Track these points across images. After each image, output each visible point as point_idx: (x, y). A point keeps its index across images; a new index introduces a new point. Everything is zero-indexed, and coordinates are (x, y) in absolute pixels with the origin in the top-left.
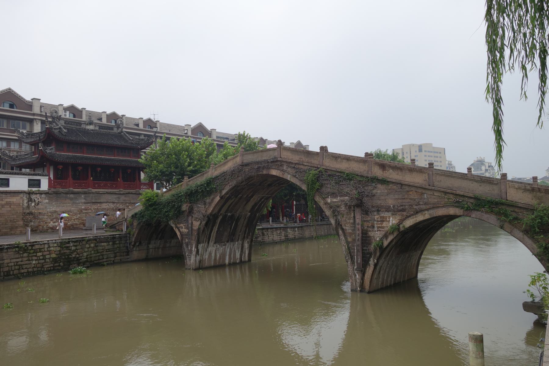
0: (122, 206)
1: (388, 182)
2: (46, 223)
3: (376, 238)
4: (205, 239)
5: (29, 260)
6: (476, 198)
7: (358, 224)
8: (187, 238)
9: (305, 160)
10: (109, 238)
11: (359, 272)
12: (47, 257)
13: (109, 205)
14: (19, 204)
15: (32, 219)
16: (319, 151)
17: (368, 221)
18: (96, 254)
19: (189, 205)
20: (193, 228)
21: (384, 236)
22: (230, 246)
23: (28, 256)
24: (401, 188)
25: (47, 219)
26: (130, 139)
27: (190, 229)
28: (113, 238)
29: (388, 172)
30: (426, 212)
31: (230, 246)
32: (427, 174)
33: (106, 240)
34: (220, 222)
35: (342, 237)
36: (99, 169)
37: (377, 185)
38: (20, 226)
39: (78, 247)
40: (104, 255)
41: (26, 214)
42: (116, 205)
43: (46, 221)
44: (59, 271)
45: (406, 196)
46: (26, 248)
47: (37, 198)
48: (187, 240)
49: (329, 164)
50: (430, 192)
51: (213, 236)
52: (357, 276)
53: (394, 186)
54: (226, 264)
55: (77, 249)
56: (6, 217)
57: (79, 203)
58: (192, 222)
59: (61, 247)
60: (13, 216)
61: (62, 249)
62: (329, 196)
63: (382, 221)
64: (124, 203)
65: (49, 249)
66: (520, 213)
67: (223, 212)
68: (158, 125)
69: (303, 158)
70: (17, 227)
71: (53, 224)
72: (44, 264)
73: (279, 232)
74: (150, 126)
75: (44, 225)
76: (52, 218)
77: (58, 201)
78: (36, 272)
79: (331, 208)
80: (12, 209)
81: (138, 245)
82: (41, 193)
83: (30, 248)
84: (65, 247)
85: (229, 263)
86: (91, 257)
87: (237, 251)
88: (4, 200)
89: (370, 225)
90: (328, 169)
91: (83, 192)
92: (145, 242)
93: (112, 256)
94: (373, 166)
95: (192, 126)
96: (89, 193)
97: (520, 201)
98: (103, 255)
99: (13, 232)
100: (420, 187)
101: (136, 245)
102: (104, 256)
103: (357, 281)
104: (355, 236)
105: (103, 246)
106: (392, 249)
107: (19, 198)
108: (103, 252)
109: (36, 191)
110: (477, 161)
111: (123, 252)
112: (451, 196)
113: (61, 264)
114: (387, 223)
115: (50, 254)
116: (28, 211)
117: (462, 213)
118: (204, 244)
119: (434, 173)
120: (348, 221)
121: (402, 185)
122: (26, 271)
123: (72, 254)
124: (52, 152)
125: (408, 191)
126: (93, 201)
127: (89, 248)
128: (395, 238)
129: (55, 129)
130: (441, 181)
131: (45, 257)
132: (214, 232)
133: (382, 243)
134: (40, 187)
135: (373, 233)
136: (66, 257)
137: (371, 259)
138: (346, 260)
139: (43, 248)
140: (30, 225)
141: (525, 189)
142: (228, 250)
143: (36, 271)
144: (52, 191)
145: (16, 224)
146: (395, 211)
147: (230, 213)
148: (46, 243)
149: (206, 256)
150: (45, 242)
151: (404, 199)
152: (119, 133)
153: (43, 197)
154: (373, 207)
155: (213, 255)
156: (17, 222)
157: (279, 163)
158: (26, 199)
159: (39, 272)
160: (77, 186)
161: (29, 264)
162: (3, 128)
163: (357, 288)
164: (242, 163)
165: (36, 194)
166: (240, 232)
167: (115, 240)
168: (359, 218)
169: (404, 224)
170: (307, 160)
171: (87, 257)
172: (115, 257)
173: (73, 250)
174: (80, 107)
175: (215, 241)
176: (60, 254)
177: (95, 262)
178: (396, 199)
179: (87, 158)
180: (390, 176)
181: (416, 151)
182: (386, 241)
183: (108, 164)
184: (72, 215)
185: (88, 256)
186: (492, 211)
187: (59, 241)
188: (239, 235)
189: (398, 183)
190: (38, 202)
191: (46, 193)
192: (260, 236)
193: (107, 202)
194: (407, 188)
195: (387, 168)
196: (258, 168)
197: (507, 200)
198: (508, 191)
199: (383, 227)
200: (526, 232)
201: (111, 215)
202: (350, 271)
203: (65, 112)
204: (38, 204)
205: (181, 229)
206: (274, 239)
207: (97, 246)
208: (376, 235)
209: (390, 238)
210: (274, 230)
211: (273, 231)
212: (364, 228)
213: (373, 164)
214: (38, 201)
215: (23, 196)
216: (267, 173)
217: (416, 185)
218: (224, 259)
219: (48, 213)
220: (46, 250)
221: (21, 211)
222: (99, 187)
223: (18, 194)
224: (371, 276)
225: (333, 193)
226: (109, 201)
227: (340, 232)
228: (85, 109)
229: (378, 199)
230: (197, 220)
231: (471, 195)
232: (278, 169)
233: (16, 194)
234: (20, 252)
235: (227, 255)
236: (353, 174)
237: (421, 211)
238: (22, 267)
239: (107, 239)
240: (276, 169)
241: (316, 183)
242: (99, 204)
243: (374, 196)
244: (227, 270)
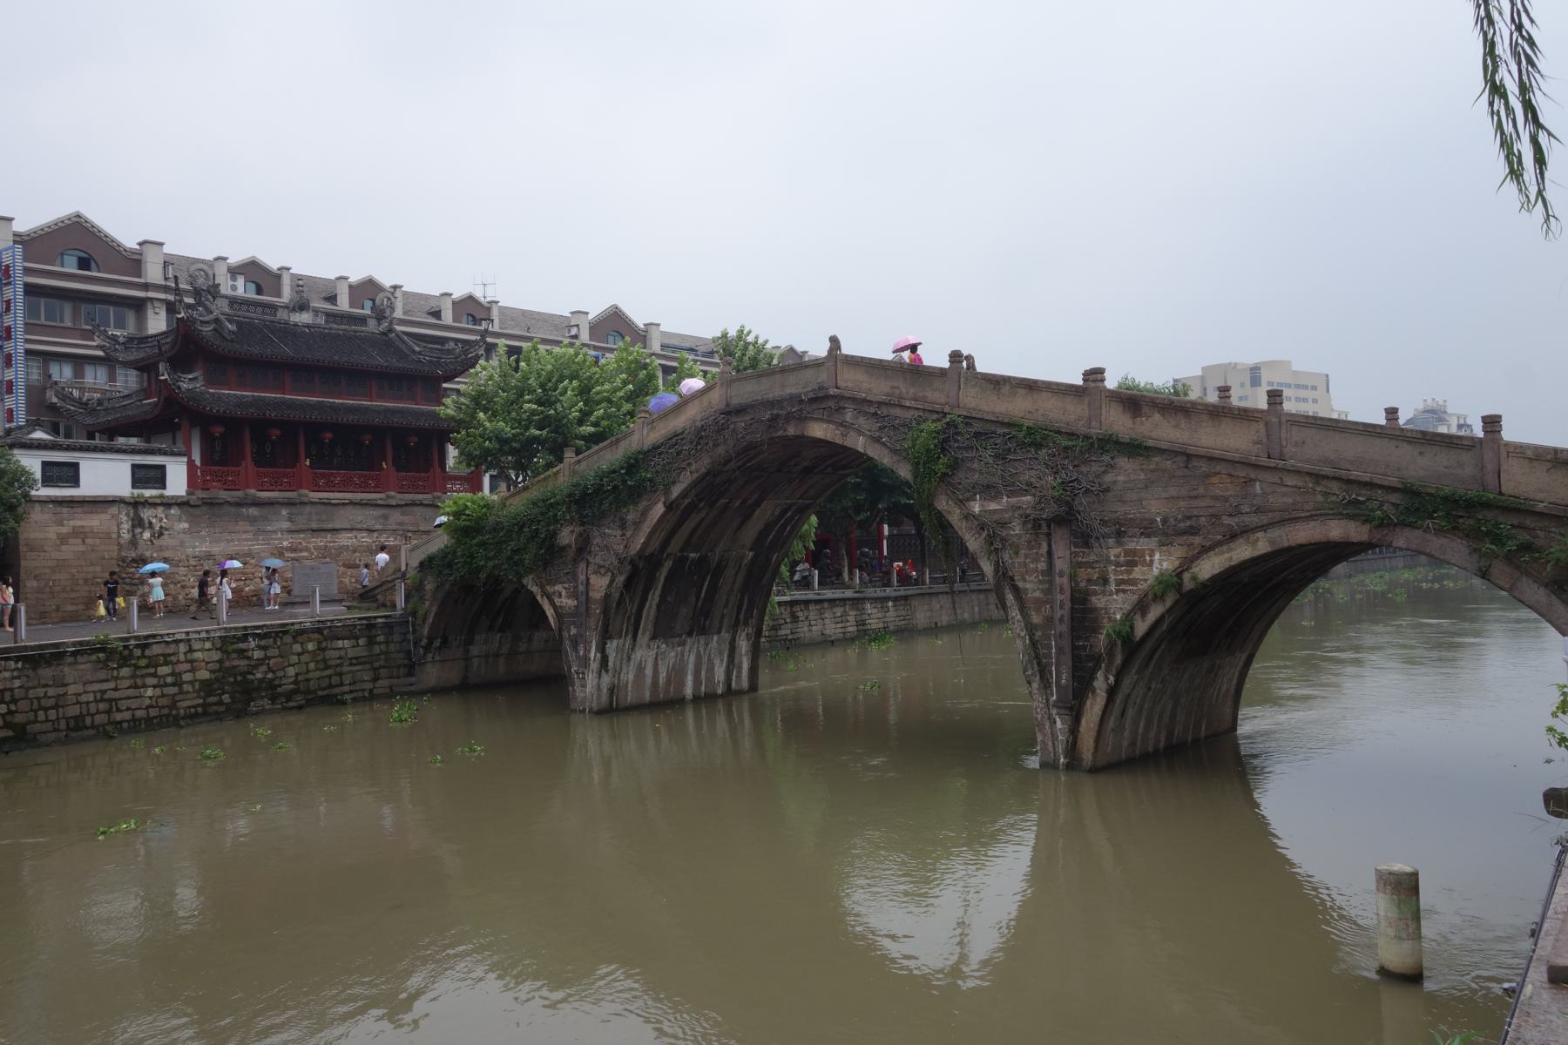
1: (1147, 448)
2: (183, 587)
3: (1114, 613)
4: (625, 625)
5: (136, 687)
6: (1407, 491)
7: (1061, 575)
8: (574, 623)
9: (907, 393)
10: (358, 627)
11: (1063, 711)
12: (187, 677)
14: (108, 536)
16: (946, 364)
17: (1089, 565)
18: (323, 670)
19: (578, 529)
20: (591, 594)
21: (1137, 605)
22: (696, 646)
23: (133, 676)
24: (1187, 467)
26: (414, 351)
27: (583, 598)
28: (370, 626)
29: (1147, 419)
30: (1260, 535)
31: (698, 648)
32: (1261, 426)
33: (349, 632)
34: (667, 578)
35: (1015, 613)
37: (1117, 460)
39: (270, 653)
40: (346, 673)
43: (183, 581)
44: (219, 717)
45: (1201, 490)
46: (126, 652)
48: (573, 631)
49: (973, 401)
50: (1273, 478)
51: (647, 617)
52: (1059, 724)
53: (1167, 460)
54: (687, 697)
55: (269, 658)
56: (74, 571)
58: (588, 579)
59: (223, 652)
60: (91, 569)
61: (225, 656)
63: (1132, 564)
65: (189, 656)
66: (1538, 532)
67: (675, 546)
68: (495, 314)
69: (901, 386)
72: (176, 698)
73: (839, 611)
74: (472, 316)
75: (179, 594)
77: (214, 527)
78: (155, 721)
79: (983, 529)
80: (90, 549)
81: (440, 648)
82: (168, 504)
83: (138, 652)
84: (235, 651)
85: (694, 696)
86: (308, 680)
87: (717, 662)
88: (65, 522)
89: (1096, 575)
90: (974, 415)
91: (286, 501)
92: (458, 638)
93: (366, 679)
94: (1103, 407)
95: (590, 317)
97: (1540, 496)
98: (340, 675)
100: (1243, 463)
101: (434, 645)
102: (344, 677)
103: (1058, 737)
104: (1051, 607)
105: (340, 649)
106: (1159, 645)
108: (341, 665)
109: (155, 497)
110: (1425, 412)
111: (399, 667)
112: (1335, 487)
113: (226, 698)
115: (193, 670)
116: (133, 555)
117: (1366, 536)
118: (621, 641)
119: (1283, 420)
120: (1031, 565)
121: (1189, 457)
122: (127, 715)
123: (254, 672)
124: (196, 388)
125: (1207, 476)
126: (314, 526)
127: (302, 654)
128: (1168, 611)
129: (201, 322)
130: (1303, 443)
131: (181, 678)
132: (650, 607)
133: (1132, 628)
134: (164, 487)
136: (239, 678)
137: (1100, 675)
138: (1027, 677)
139: (173, 654)
140: (139, 593)
141: (1556, 459)
142: (692, 659)
143: (155, 717)
144: (198, 498)
146: (1167, 533)
148: (181, 641)
149: (628, 673)
150: (178, 637)
151: (1196, 497)
152: (383, 334)
153: (173, 515)
154: (1103, 523)
155: (649, 671)
157: (831, 403)
159: (164, 719)
161: (136, 697)
162: (61, 325)
163: (1056, 759)
164: (728, 405)
165: (155, 505)
166: (726, 606)
167: (374, 632)
168: (1063, 555)
169: (1195, 570)
170: (912, 391)
171: (297, 678)
172: (375, 680)
173: (258, 660)
174: (273, 264)
175: (654, 632)
176: (219, 670)
177: (320, 693)
178: (1173, 497)
179: (291, 405)
180: (1152, 434)
181: (1242, 385)
182: (1143, 621)
185: (300, 678)
186: (1455, 528)
187: (218, 634)
188: (723, 616)
189: (1176, 453)
190: (161, 527)
191: (181, 503)
192: (786, 623)
193: (352, 529)
194: (1204, 467)
195: (1145, 409)
196: (774, 419)
197: (1501, 493)
198: (1504, 467)
199: (1133, 582)
200: (1556, 587)
202: (1039, 710)
203: (234, 278)
204: (161, 534)
205: (556, 600)
206: (827, 632)
207: (324, 650)
208: (1114, 605)
209: (1155, 612)
210: (826, 605)
211: (823, 608)
212: (1077, 584)
213: (1103, 397)
214: (159, 525)
215: (120, 513)
216: (798, 433)
217: (1230, 455)
218: (682, 684)
219: (188, 561)
220: (182, 657)
221: (115, 555)
222: (330, 487)
224: (1097, 723)
225: (988, 487)
226: (359, 526)
227: (1010, 597)
228: (288, 269)
230: (603, 571)
231: (1393, 481)
232: (829, 422)
234: (110, 664)
235: (689, 672)
236: (1046, 430)
237: (1246, 532)
238: (116, 704)
239: (351, 628)
240: (822, 420)
241: (939, 458)
243: (1107, 490)
244: (690, 713)
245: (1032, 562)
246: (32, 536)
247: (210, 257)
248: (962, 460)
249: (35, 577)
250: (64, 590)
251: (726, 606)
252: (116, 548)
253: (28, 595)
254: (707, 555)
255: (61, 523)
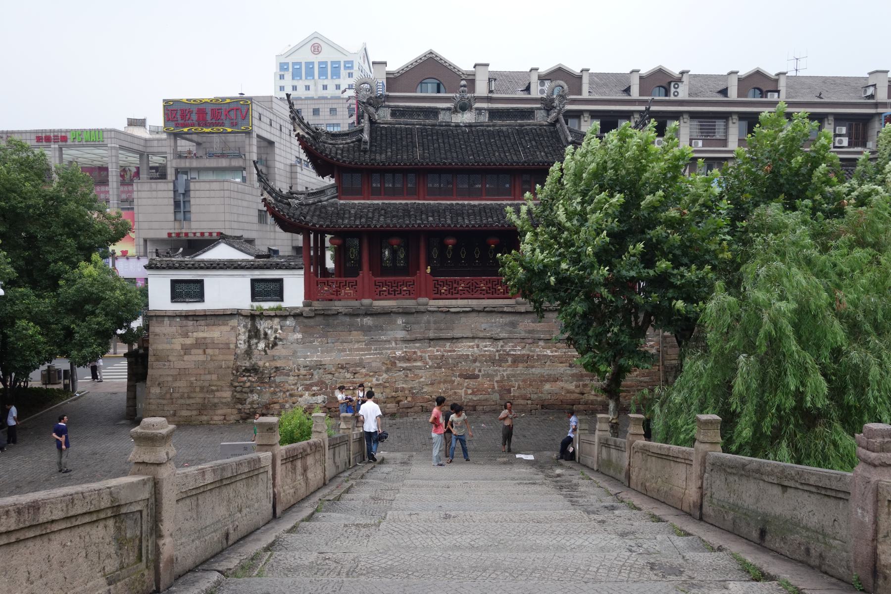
0: (524, 348)
2: (291, 395)
13: (481, 347)
14: (227, 346)
15: (255, 385)
25: (296, 384)
36: (451, 242)
38: (222, 403)
41: (241, 371)
42: (502, 346)
47: (271, 328)
56: (193, 379)
57: (389, 341)
60: (208, 377)
64: (530, 341)
70: (215, 405)
71: (309, 398)
75: (287, 402)
76: (308, 382)
80: (209, 358)
82: (283, 315)
88: (190, 334)
91: (401, 310)
96: (417, 312)
99: (204, 418)
107: (228, 328)
116: (248, 364)
124: (321, 201)
126: (431, 335)
134: (282, 300)
140: (249, 400)
145: (214, 397)
156: (218, 391)
158: (245, 333)
160: (386, 293)
165: (270, 317)
174: (576, 69)
183: (467, 226)
184: (366, 375)
190: (276, 338)
191: (297, 315)
193: (473, 338)
201: (483, 375)
203: (542, 84)
204: (275, 344)
219: (299, 370)
221: (231, 364)
222: (453, 294)
223: (227, 318)
226: (481, 335)
228: (588, 70)
233: (222, 318)
242: (448, 344)
246: (160, 347)
247: (627, 71)
249: (159, 384)
250: (182, 397)
252: (232, 357)
253: (151, 401)
255: (186, 335)
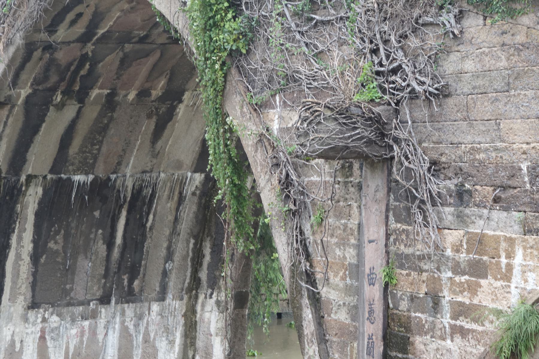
22: (118, 319)
31: (123, 322)
34: (37, 214)
51: (16, 274)
62: (273, 96)
87: (162, 345)
89: (424, 289)
114: (499, 284)
120: (338, 252)
132: (18, 257)
135: (434, 346)
147: (87, 174)
166: (169, 257)
175: (33, 296)
188: (165, 274)
229: (465, 120)
245: (338, 245)
248: (258, 22)
251: (169, 257)
254: (109, 179)
